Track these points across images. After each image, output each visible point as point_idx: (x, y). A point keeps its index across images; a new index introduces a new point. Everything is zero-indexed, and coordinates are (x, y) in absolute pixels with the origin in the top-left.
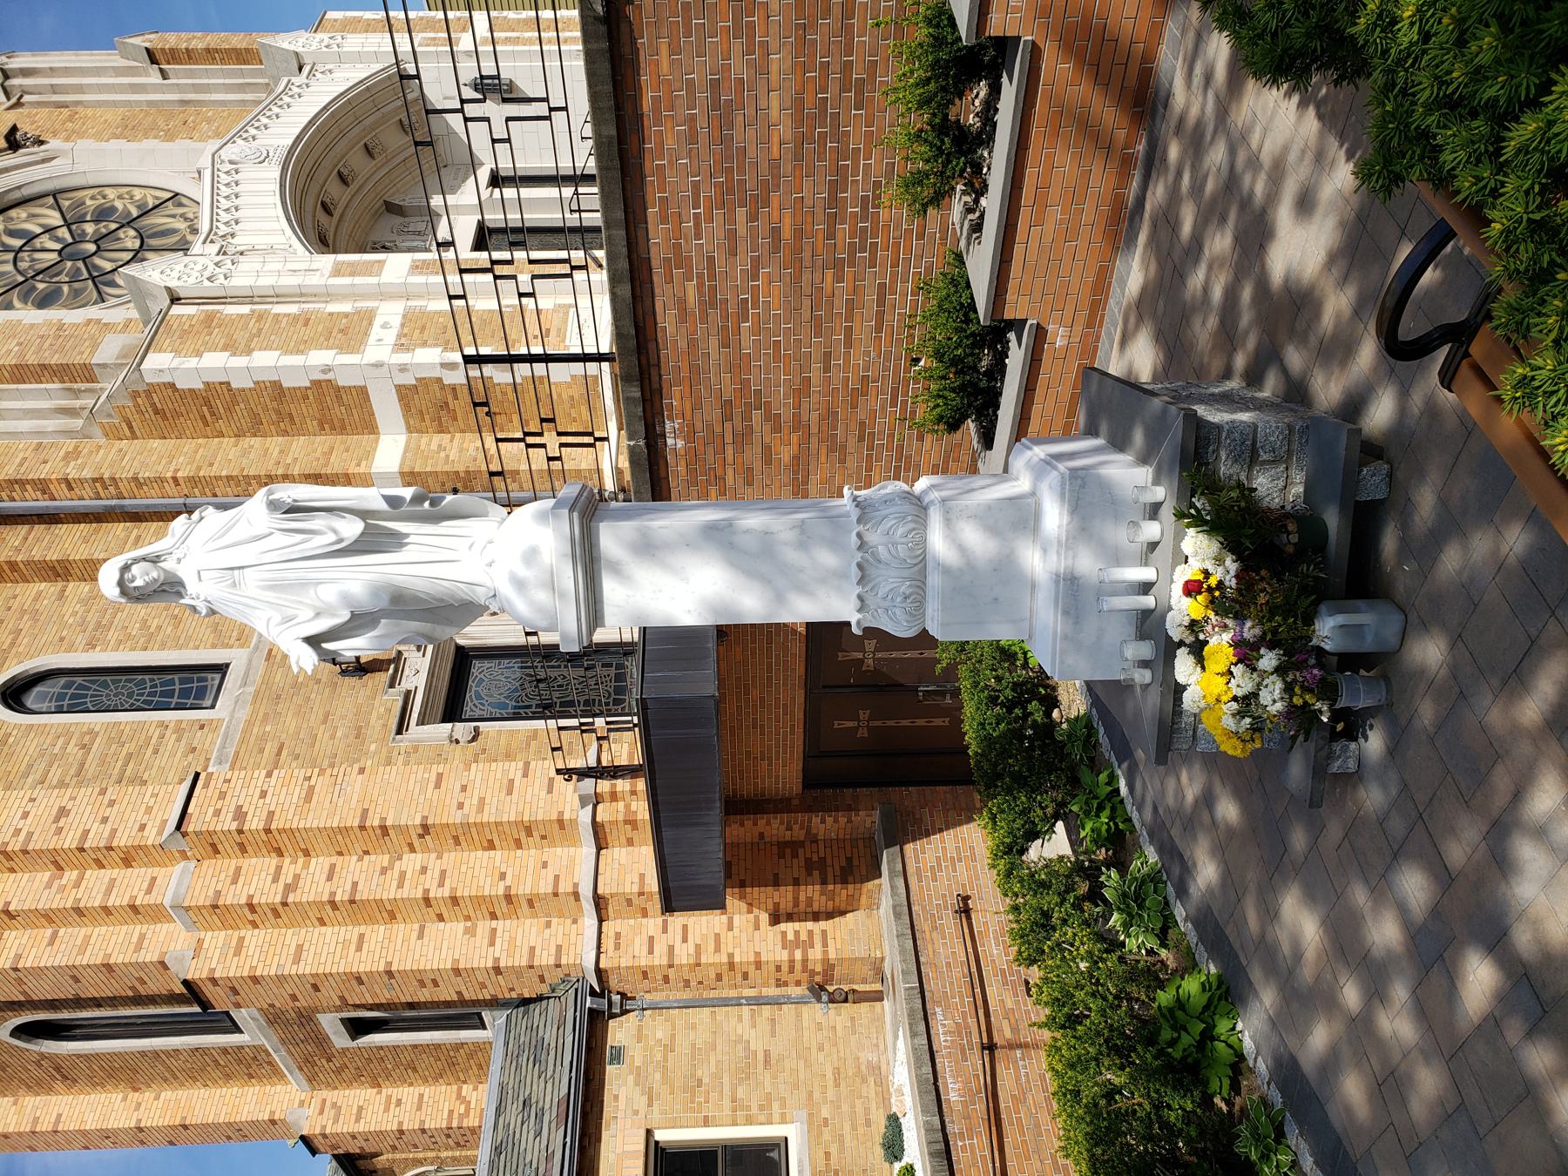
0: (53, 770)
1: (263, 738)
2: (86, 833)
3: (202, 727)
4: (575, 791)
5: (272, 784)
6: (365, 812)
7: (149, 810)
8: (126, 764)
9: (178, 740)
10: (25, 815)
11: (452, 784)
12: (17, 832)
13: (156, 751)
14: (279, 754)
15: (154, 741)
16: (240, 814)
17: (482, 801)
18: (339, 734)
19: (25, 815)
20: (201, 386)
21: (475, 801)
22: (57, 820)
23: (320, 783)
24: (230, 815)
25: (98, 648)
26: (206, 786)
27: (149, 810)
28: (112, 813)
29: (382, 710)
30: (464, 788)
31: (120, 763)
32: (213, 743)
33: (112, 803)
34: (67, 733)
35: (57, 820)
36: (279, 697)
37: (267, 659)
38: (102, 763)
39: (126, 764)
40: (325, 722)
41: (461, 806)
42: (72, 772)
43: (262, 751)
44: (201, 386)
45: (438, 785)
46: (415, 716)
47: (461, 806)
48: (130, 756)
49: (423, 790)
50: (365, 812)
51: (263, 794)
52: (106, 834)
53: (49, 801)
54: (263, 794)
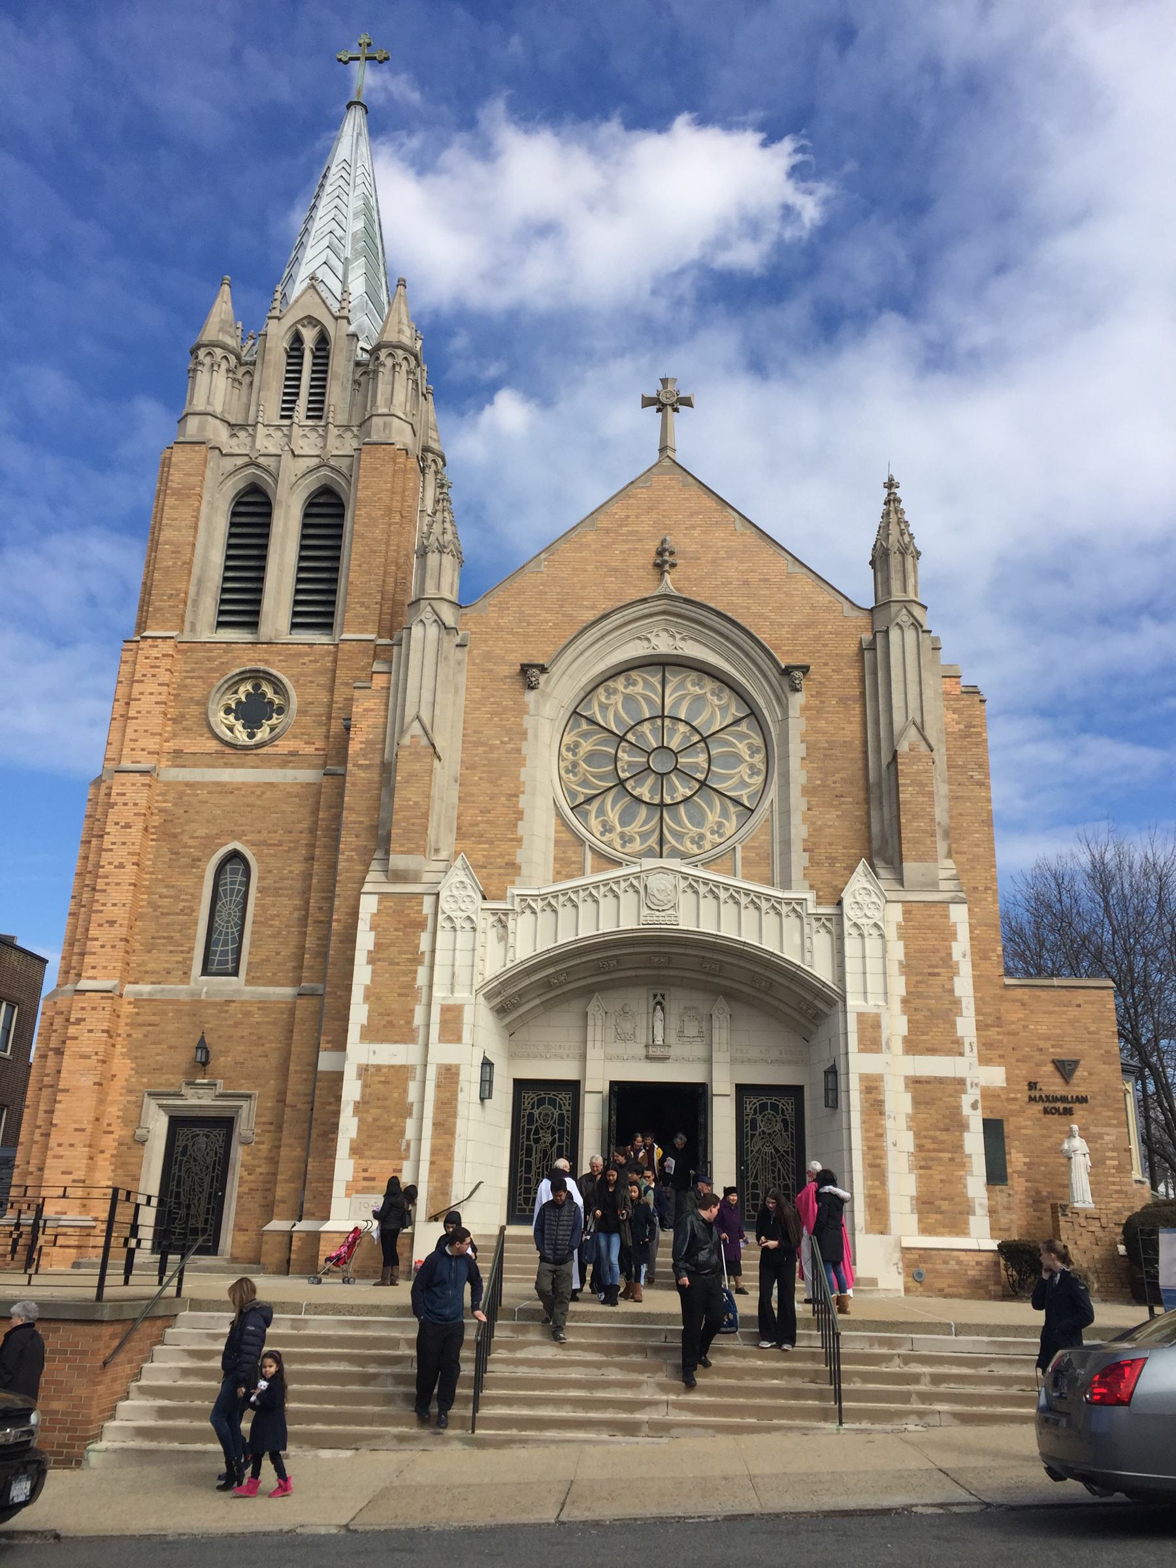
0: (169, 900)
1: (164, 1013)
2: (96, 939)
3: (185, 973)
4: (26, 1213)
5: (97, 1035)
6: (67, 1091)
7: (105, 968)
8: (164, 938)
9: (178, 962)
10: (114, 905)
11: (78, 1138)
12: (104, 905)
13: (171, 952)
14: (150, 1025)
15: (180, 948)
16: (79, 1021)
17: (61, 1157)
18: (159, 1058)
19: (114, 905)
20: (373, 933)
21: (62, 1153)
22: (107, 922)
23: (93, 1062)
24: (80, 1016)
25: (259, 895)
26: (102, 998)
27: (105, 968)
28: (108, 949)
29: (173, 1081)
30: (72, 1145)
31: (166, 934)
32: (172, 983)
33: (113, 947)
34: (196, 897)
35: (107, 922)
36: (194, 1015)
37: (226, 1001)
38: (168, 924)
39: (164, 938)
40: (170, 1047)
41: (60, 1145)
42: (165, 911)
43: (154, 1014)
44: (373, 933)
45: (76, 1130)
46: (165, 1102)
47: (60, 1145)
48: (171, 938)
49: (75, 1122)
50: (67, 1091)
51: (90, 1031)
52: (94, 950)
53: (120, 914)
54: (90, 1031)
